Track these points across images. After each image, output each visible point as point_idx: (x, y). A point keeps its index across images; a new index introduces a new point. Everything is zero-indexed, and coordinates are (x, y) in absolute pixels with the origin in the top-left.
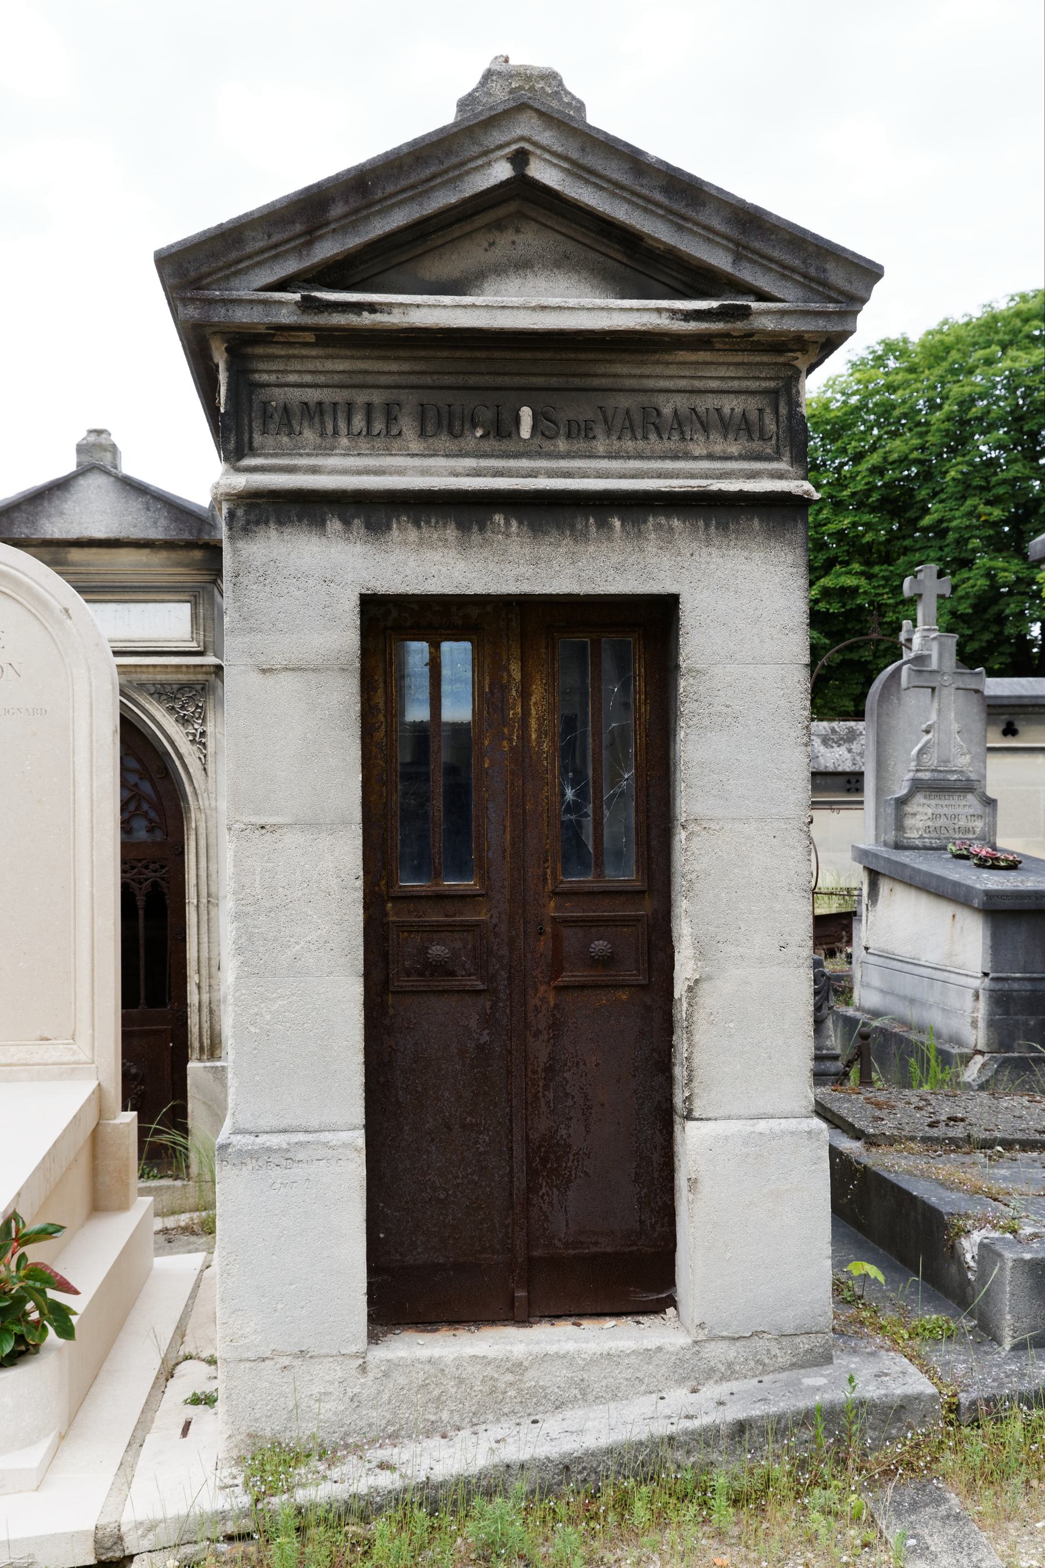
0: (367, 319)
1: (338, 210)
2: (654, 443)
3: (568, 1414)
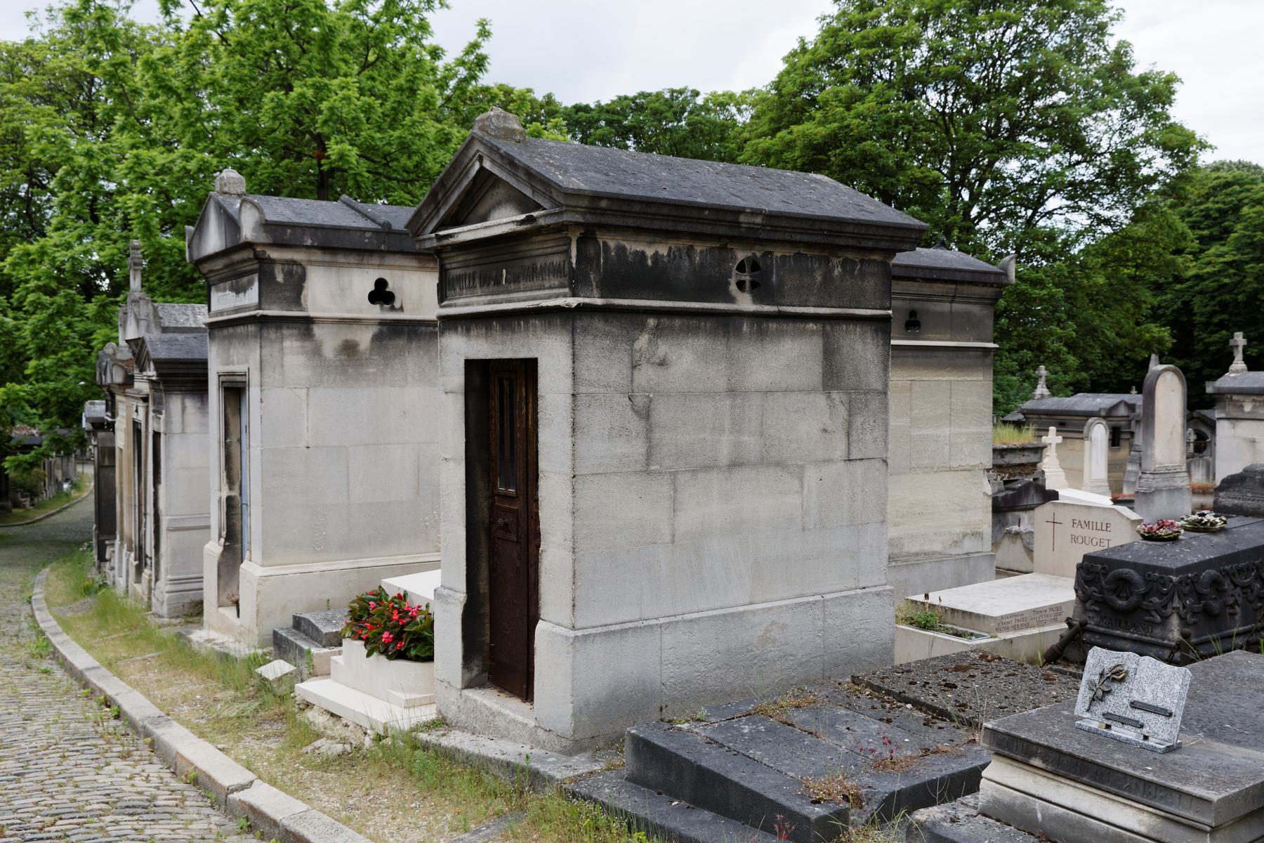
0: (451, 240)
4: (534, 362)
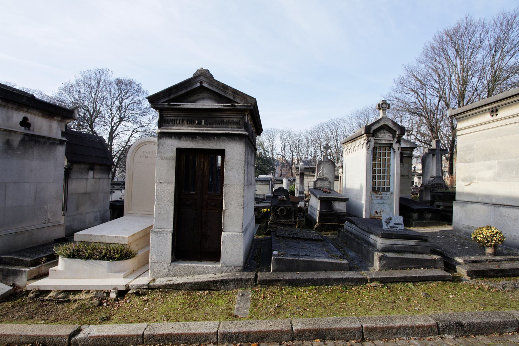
0: (177, 107)
2: (223, 125)
4: (224, 150)
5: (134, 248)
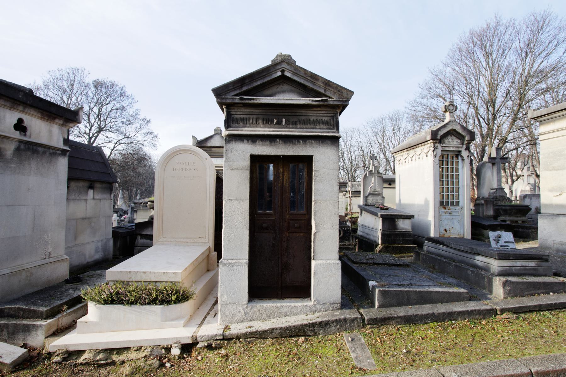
0: (252, 102)
1: (247, 81)
3: (287, 317)
5: (186, 286)
